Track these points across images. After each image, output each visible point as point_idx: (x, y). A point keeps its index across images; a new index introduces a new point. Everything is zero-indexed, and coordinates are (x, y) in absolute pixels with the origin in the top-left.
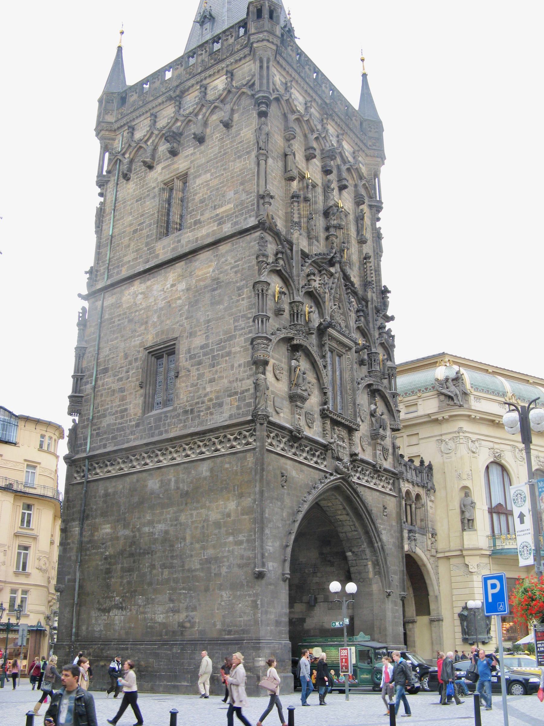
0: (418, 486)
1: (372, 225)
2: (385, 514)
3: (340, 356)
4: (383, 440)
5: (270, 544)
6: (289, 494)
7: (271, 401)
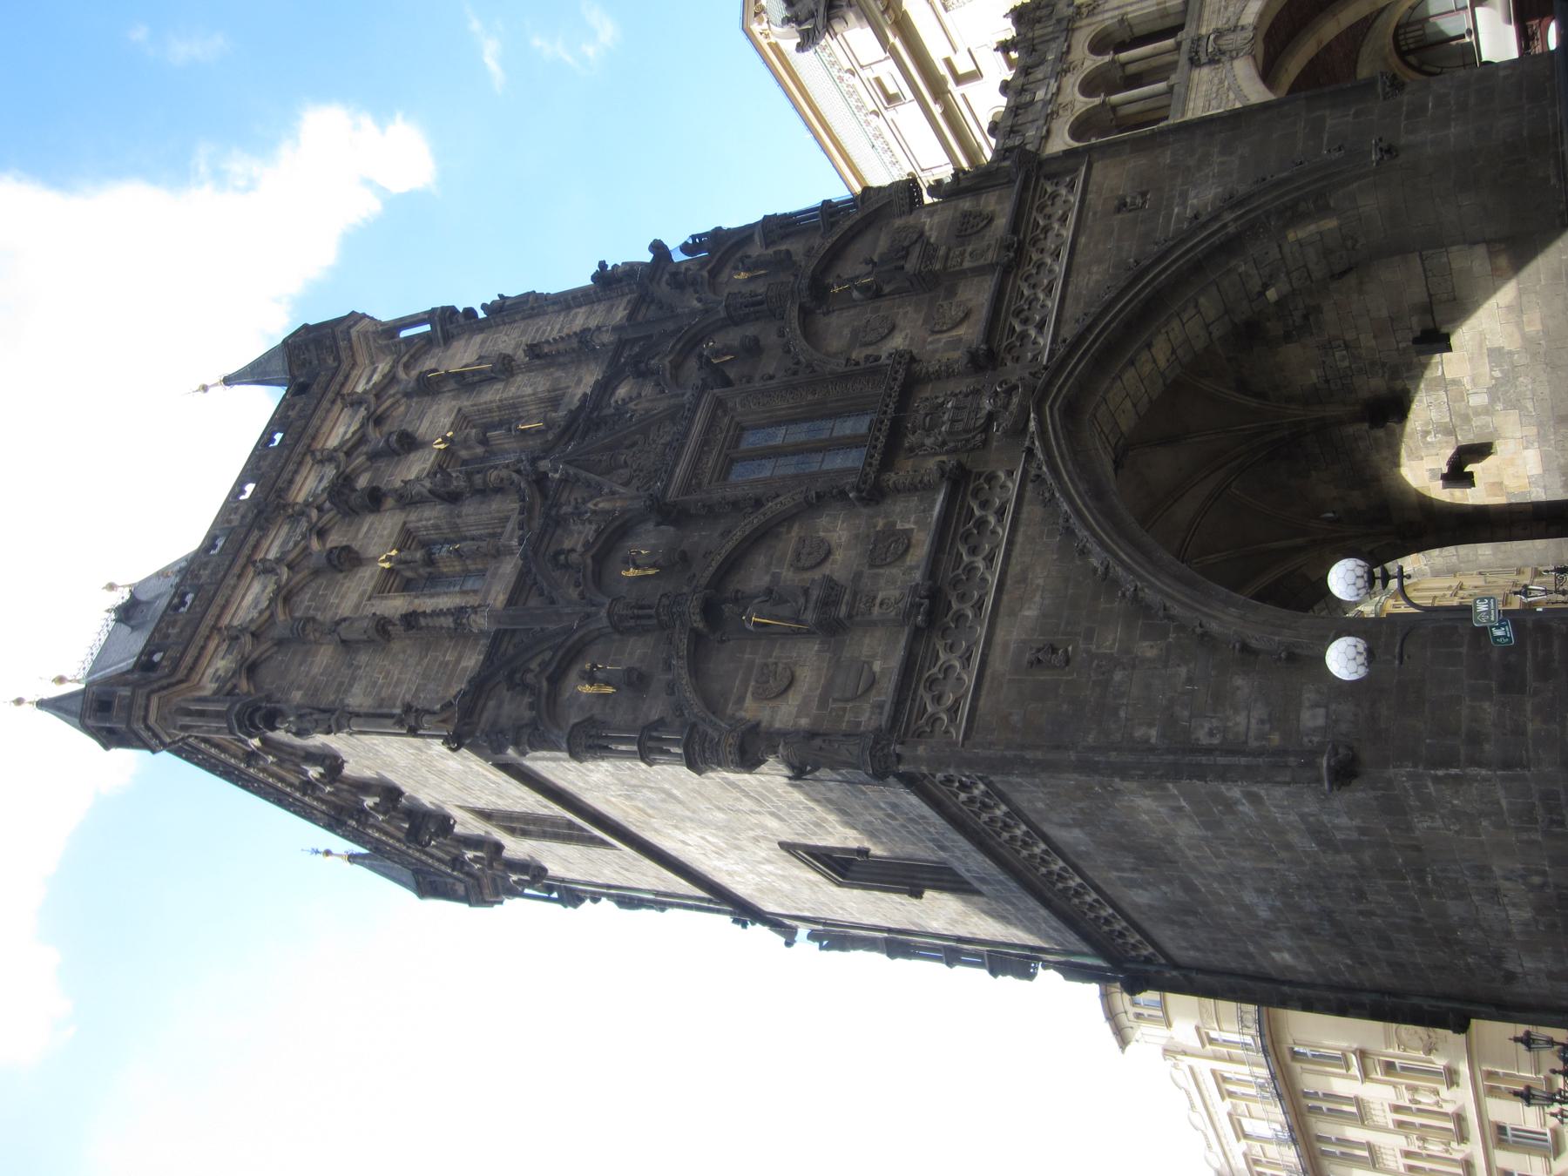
0: (1068, 52)
1: (481, 330)
2: (1139, 201)
3: (742, 429)
4: (936, 250)
5: (1241, 719)
6: (1089, 635)
7: (844, 710)
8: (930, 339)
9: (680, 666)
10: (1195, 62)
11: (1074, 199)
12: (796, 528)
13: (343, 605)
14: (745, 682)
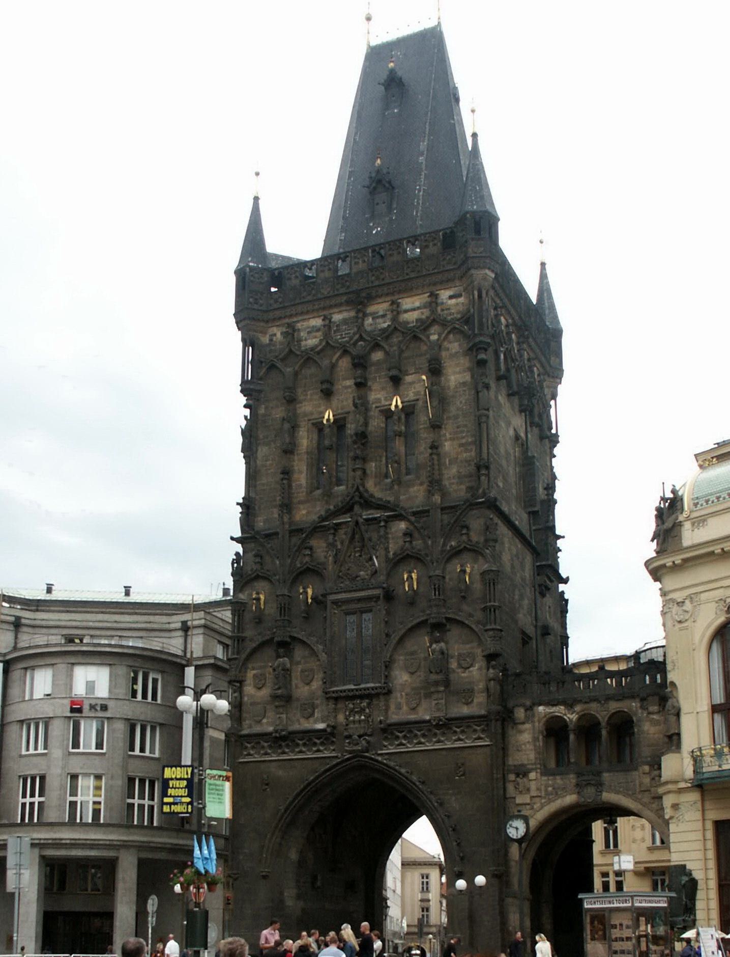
8: (403, 694)
9: (260, 639)
10: (579, 774)
11: (469, 743)
12: (318, 663)
13: (306, 403)
14: (261, 668)
